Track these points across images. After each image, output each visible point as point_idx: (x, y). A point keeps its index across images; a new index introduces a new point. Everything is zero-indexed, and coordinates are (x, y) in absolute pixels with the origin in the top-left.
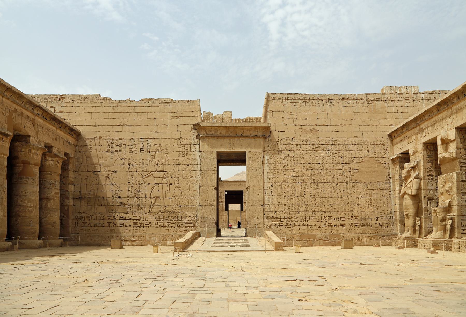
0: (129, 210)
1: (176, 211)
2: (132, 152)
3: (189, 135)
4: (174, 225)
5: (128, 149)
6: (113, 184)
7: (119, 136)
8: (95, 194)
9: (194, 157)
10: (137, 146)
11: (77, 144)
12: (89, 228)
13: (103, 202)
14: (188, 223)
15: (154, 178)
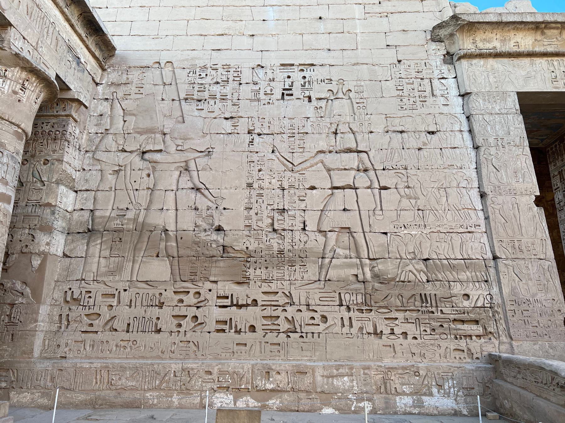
0: (251, 271)
1: (412, 277)
2: (259, 100)
3: (423, 55)
4: (411, 329)
5: (246, 91)
6: (198, 189)
7: (220, 59)
8: (141, 219)
9: (445, 110)
10: (272, 84)
11: (101, 79)
12: (108, 336)
13: (163, 245)
14: (463, 322)
15: (329, 170)
